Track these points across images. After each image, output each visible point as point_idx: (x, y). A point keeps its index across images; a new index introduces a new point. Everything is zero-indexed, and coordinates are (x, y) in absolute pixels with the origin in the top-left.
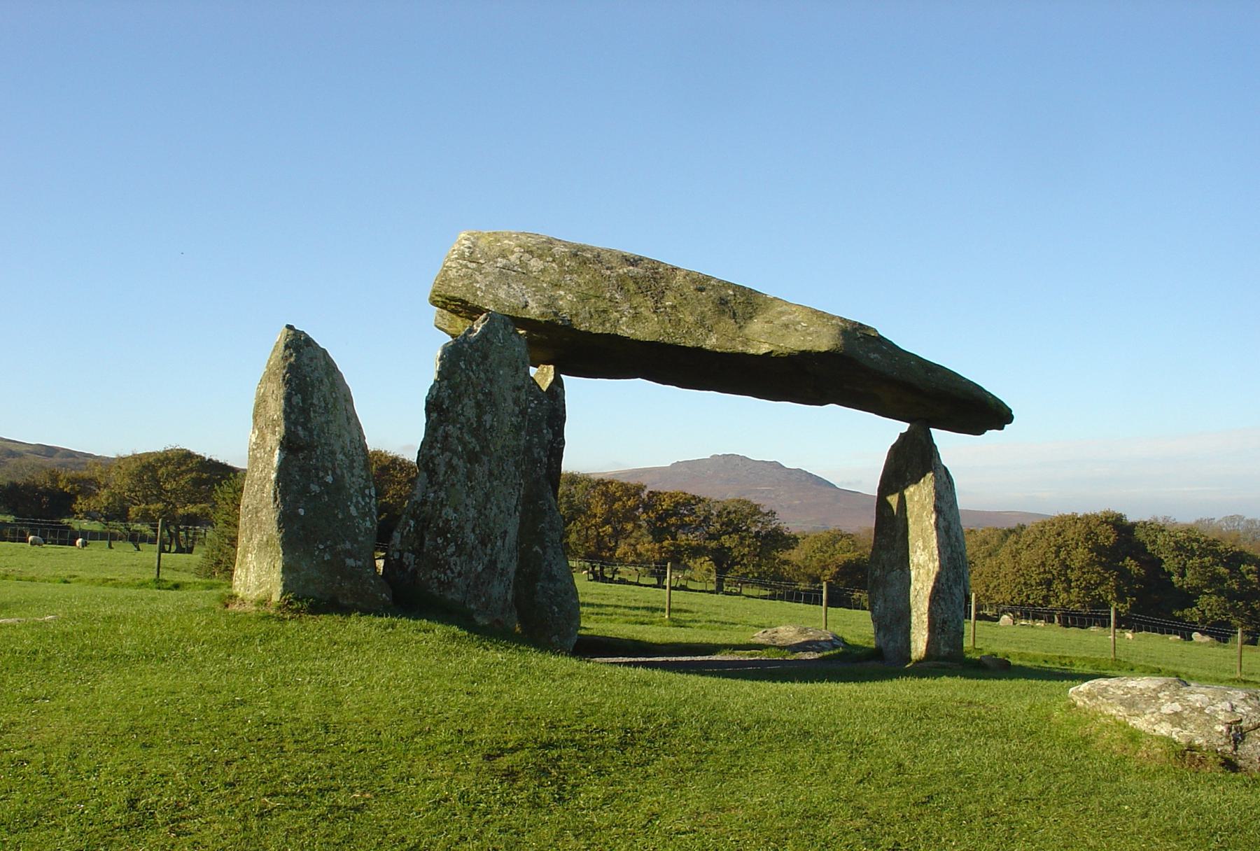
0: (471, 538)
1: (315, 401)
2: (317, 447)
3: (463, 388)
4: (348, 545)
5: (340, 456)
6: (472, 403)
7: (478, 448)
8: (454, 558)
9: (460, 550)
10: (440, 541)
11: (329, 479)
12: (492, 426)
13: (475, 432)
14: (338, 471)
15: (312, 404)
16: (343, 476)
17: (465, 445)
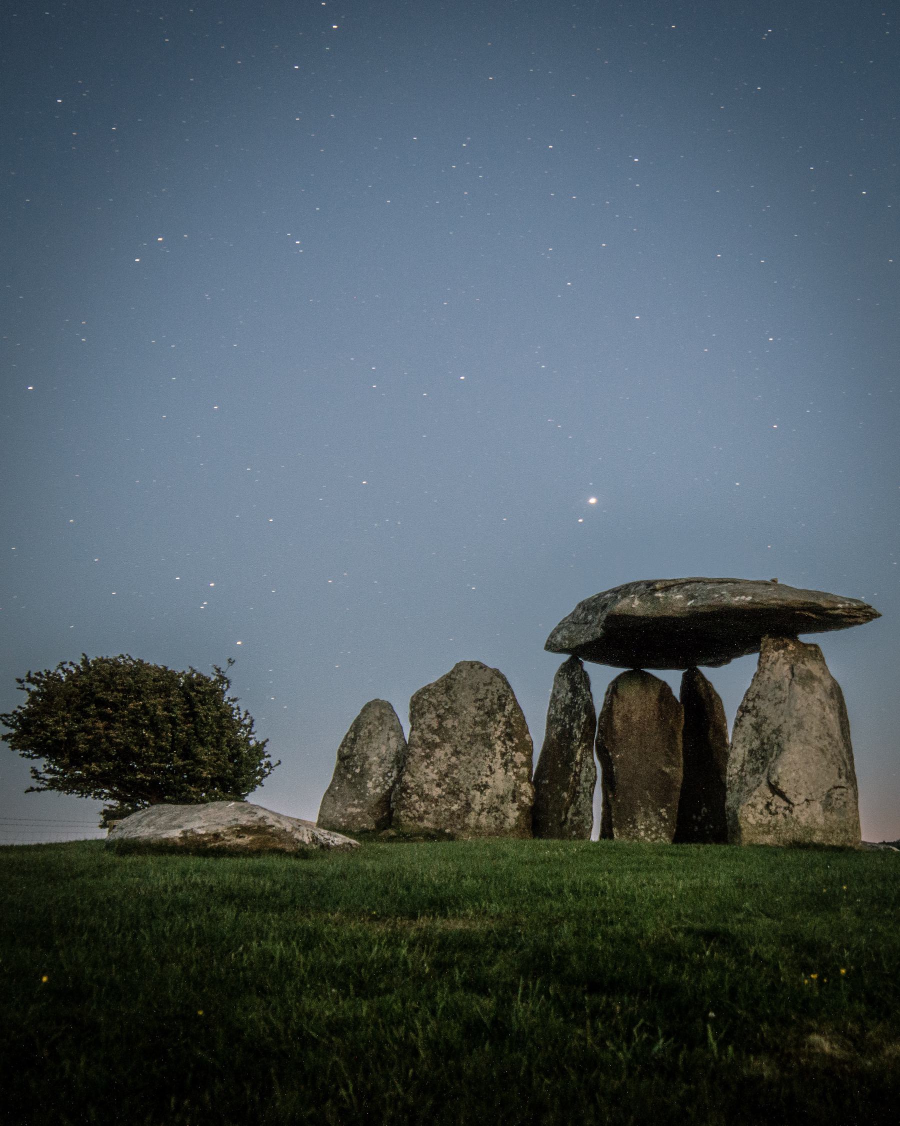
0: (436, 792)
1: (362, 734)
2: (355, 756)
3: (425, 710)
4: (356, 802)
5: (374, 758)
6: (434, 715)
7: (438, 740)
8: (419, 803)
9: (424, 797)
10: (404, 795)
11: (358, 771)
12: (453, 726)
13: (434, 732)
14: (367, 766)
15: (360, 736)
16: (370, 769)
17: (424, 741)
